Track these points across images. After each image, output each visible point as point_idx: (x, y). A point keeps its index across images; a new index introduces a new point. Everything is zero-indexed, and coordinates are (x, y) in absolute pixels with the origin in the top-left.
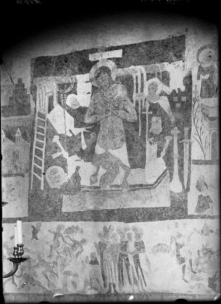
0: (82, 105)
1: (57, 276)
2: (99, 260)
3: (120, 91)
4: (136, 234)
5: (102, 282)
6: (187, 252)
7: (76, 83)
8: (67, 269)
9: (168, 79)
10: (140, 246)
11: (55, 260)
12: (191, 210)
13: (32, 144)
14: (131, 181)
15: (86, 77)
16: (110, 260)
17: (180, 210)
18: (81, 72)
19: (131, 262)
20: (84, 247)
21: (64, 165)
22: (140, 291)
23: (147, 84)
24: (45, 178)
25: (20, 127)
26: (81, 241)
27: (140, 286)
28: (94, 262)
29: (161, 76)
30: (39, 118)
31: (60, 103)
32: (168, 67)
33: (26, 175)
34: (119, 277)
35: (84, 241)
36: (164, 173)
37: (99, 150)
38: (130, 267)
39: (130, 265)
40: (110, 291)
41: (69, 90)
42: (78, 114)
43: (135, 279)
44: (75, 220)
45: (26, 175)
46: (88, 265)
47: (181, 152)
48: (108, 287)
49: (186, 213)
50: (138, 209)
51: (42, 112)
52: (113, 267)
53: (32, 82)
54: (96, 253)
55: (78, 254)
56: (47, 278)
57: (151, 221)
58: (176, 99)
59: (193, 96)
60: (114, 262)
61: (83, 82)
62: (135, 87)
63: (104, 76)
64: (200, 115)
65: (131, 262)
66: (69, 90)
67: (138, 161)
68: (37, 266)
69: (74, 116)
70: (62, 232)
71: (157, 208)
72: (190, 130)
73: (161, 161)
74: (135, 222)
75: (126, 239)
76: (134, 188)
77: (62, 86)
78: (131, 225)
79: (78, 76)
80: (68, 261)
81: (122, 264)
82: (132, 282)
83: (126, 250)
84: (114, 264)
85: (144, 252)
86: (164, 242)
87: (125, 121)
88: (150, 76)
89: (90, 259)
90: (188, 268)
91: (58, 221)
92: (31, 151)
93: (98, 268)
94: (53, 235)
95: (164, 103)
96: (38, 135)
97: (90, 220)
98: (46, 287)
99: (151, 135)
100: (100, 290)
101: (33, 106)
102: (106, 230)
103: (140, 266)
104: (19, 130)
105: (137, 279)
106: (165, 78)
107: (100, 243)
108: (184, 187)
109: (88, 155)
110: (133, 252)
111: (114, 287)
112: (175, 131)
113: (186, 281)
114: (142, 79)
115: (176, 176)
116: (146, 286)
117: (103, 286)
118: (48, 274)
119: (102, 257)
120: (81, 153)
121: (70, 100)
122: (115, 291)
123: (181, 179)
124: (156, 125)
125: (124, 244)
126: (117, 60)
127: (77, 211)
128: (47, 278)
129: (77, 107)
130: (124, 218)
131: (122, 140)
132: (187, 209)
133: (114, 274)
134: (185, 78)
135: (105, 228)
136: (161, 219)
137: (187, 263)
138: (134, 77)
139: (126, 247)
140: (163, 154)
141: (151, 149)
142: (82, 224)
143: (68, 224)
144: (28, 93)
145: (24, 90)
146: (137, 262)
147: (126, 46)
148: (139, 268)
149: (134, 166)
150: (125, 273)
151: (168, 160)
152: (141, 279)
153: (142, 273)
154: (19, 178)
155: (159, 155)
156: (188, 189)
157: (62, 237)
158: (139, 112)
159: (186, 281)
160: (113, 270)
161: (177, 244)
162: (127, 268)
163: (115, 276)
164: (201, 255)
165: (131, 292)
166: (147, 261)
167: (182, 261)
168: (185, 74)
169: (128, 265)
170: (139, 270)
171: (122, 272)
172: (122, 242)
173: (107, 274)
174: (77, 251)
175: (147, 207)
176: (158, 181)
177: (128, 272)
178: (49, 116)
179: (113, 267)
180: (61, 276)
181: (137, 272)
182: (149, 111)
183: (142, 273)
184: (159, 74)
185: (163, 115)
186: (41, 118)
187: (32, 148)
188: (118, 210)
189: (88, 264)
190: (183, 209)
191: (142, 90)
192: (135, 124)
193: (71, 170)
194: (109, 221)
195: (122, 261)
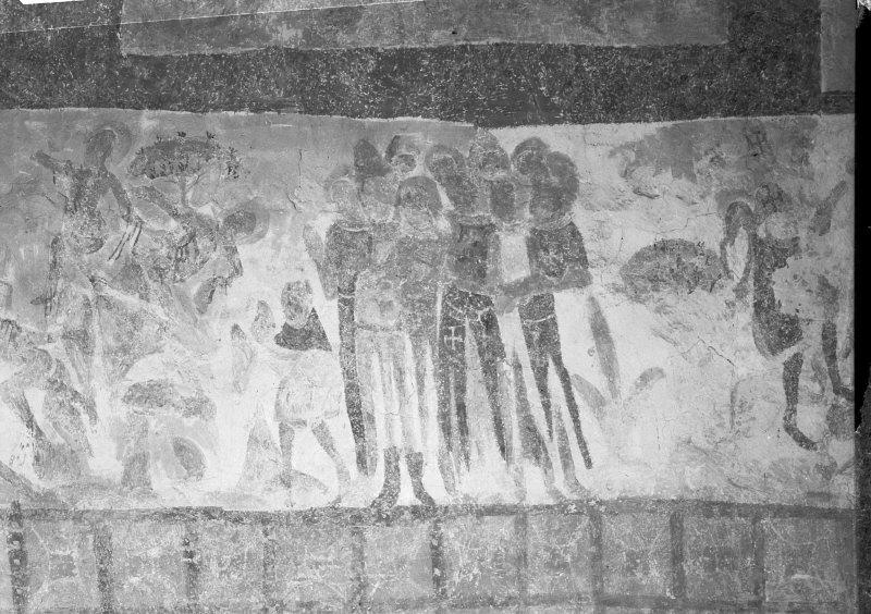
1: (91, 408)
2: (330, 319)
4: (537, 185)
6: (815, 285)
8: (144, 371)
11: (77, 323)
16: (392, 323)
17: (782, 67)
19: (511, 330)
20: (245, 251)
22: (556, 493)
26: (232, 220)
27: (557, 462)
34: (444, 416)
35: (245, 220)
38: (506, 367)
39: (503, 356)
40: (390, 492)
43: (529, 429)
44: (197, 105)
46: (266, 349)
48: (381, 467)
49: (812, 81)
50: (552, 55)
52: (409, 363)
54: (316, 285)
55: (209, 292)
56: (30, 423)
57: (619, 120)
60: (416, 336)
65: (511, 330)
70: (119, 166)
71: (654, 53)
74: (535, 122)
75: (483, 212)
78: (509, 138)
80: (149, 329)
81: (461, 347)
82: (516, 443)
83: (481, 274)
84: (415, 347)
85: (584, 282)
86: (688, 236)
89: (279, 317)
90: (816, 368)
91: (99, 102)
93: (325, 366)
94: (65, 182)
97: (278, 106)
98: (27, 471)
100: (334, 487)
103: (558, 361)
105: (543, 429)
107: (335, 231)
110: (524, 286)
111: (416, 469)
113: (803, 441)
116: (589, 463)
117: (353, 468)
118: (37, 398)
119: (347, 307)
122: (420, 492)
125: (472, 237)
127: (207, 50)
128: (30, 423)
130: (472, 103)
132: (814, 61)
133: (415, 400)
136: (677, 109)
139: (484, 255)
142: (229, 124)
143: (147, 121)
146: (544, 339)
148: (552, 369)
150: (475, 392)
152: (563, 431)
153: (570, 399)
157: (118, 192)
159: (803, 441)
160: (410, 381)
161: (757, 245)
162: (490, 369)
163: (423, 411)
165: (509, 499)
166: (600, 330)
169: (492, 352)
170: (554, 381)
171: (461, 389)
172: (463, 229)
173: (378, 402)
174: (206, 275)
175: (602, 43)
177: (493, 390)
179: (409, 363)
180: (110, 407)
181: (543, 390)
183: (570, 399)
188: (441, 53)
189: (272, 344)
190: (793, 58)
194: (388, 114)
195: (461, 331)
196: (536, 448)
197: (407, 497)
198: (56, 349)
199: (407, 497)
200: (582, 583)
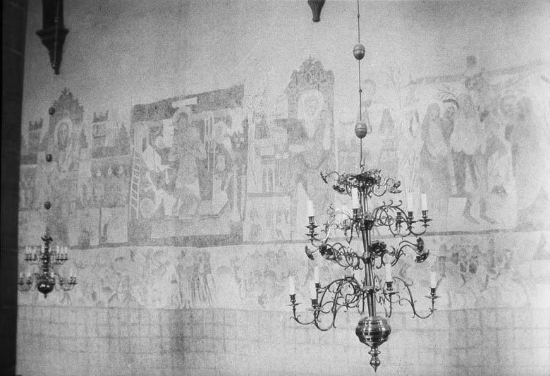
0: (167, 145)
2: (178, 280)
3: (195, 133)
5: (180, 299)
7: (162, 127)
9: (231, 123)
10: (208, 269)
12: (246, 236)
14: (201, 212)
15: (170, 121)
18: (166, 117)
19: (201, 279)
21: (153, 198)
23: (214, 126)
24: (139, 209)
28: (174, 281)
29: (225, 120)
31: (151, 144)
32: (231, 112)
33: (126, 206)
35: (168, 263)
36: (226, 204)
37: (179, 185)
41: (157, 133)
42: (164, 152)
43: (203, 296)
45: (126, 206)
47: (239, 188)
58: (236, 140)
59: (249, 138)
61: (168, 125)
62: (206, 130)
63: (183, 120)
64: (254, 153)
66: (157, 133)
67: (208, 197)
68: (135, 284)
69: (161, 155)
72: (246, 168)
73: (224, 194)
76: (203, 217)
77: (152, 130)
78: (202, 249)
79: (164, 121)
85: (211, 273)
87: (197, 159)
88: (218, 119)
89: (171, 279)
92: (130, 186)
95: (227, 144)
99: (218, 172)
101: (132, 146)
102: (183, 254)
106: (228, 121)
108: (241, 217)
109: (171, 188)
112: (235, 168)
114: (211, 123)
115: (235, 208)
120: (166, 187)
121: (157, 142)
123: (240, 209)
124: (221, 165)
126: (193, 107)
129: (164, 147)
131: (195, 176)
134: (244, 122)
135: (182, 252)
137: (243, 282)
138: (205, 121)
140: (226, 188)
141: (217, 184)
143: (155, 249)
145: (126, 133)
147: (200, 94)
149: (204, 198)
150: (196, 291)
151: (230, 192)
155: (222, 188)
156: (244, 219)
158: (208, 151)
164: (253, 275)
166: (213, 279)
167: (239, 281)
168: (244, 118)
170: (207, 290)
173: (184, 292)
176: (222, 212)
178: (143, 155)
182: (216, 150)
184: (224, 118)
185: (226, 154)
191: (211, 133)
192: (205, 161)
193: (158, 202)
196: (204, 299)
197: (188, 307)
198: (144, 283)
199: (188, 307)
200: (211, 321)
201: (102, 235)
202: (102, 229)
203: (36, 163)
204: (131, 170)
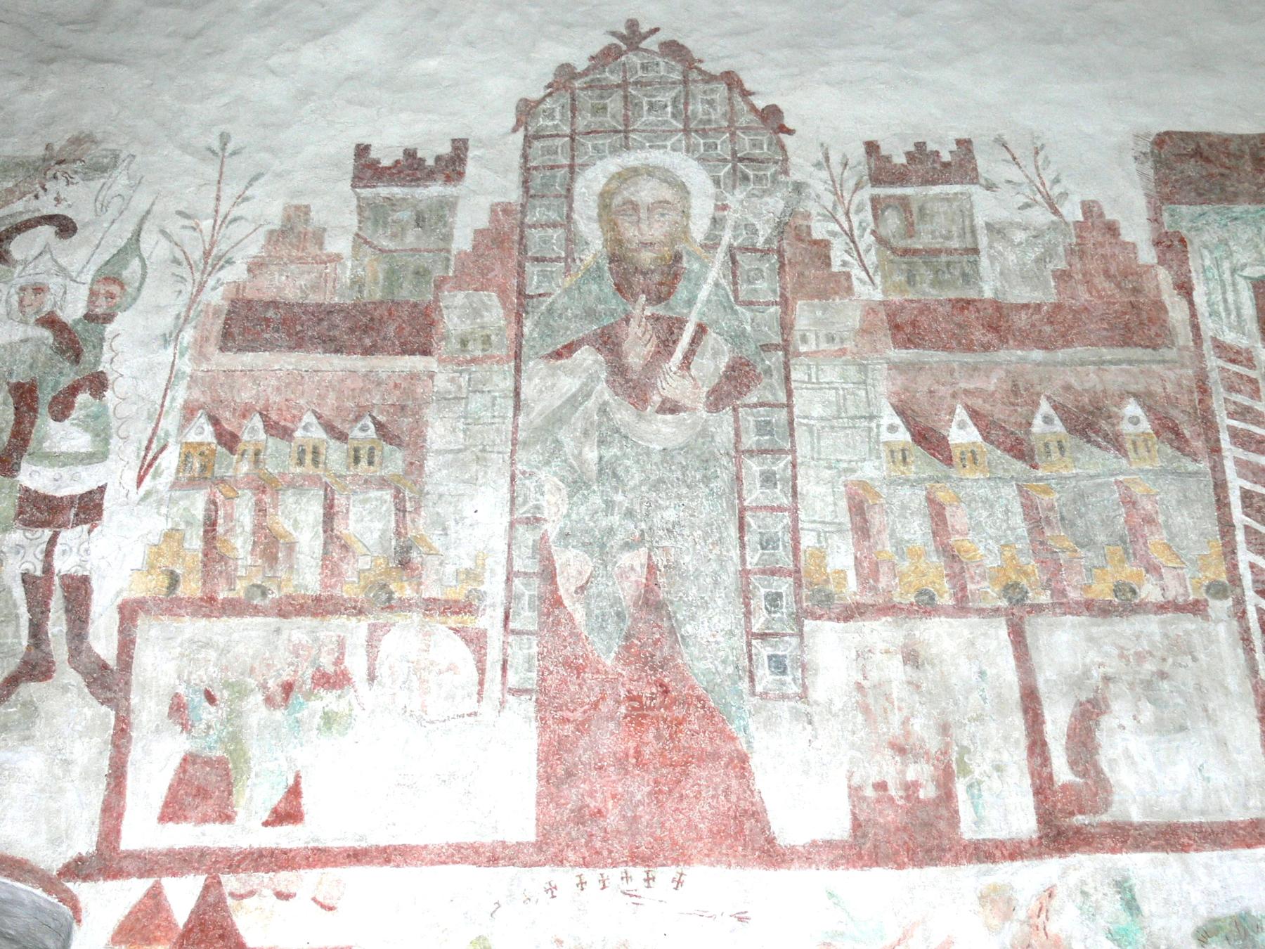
13: (1217, 468)
25: (1136, 396)
30: (1221, 363)
33: (1220, 607)
51: (1229, 337)
53: (1155, 220)
92: (1222, 504)
96: (1235, 434)
101: (1177, 313)
104: (1132, 408)
144: (1147, 255)
154: (1188, 624)
186: (1233, 361)
187: (1220, 486)
201: (1062, 772)
202: (1057, 720)
203: (426, 352)
204: (1208, 424)
